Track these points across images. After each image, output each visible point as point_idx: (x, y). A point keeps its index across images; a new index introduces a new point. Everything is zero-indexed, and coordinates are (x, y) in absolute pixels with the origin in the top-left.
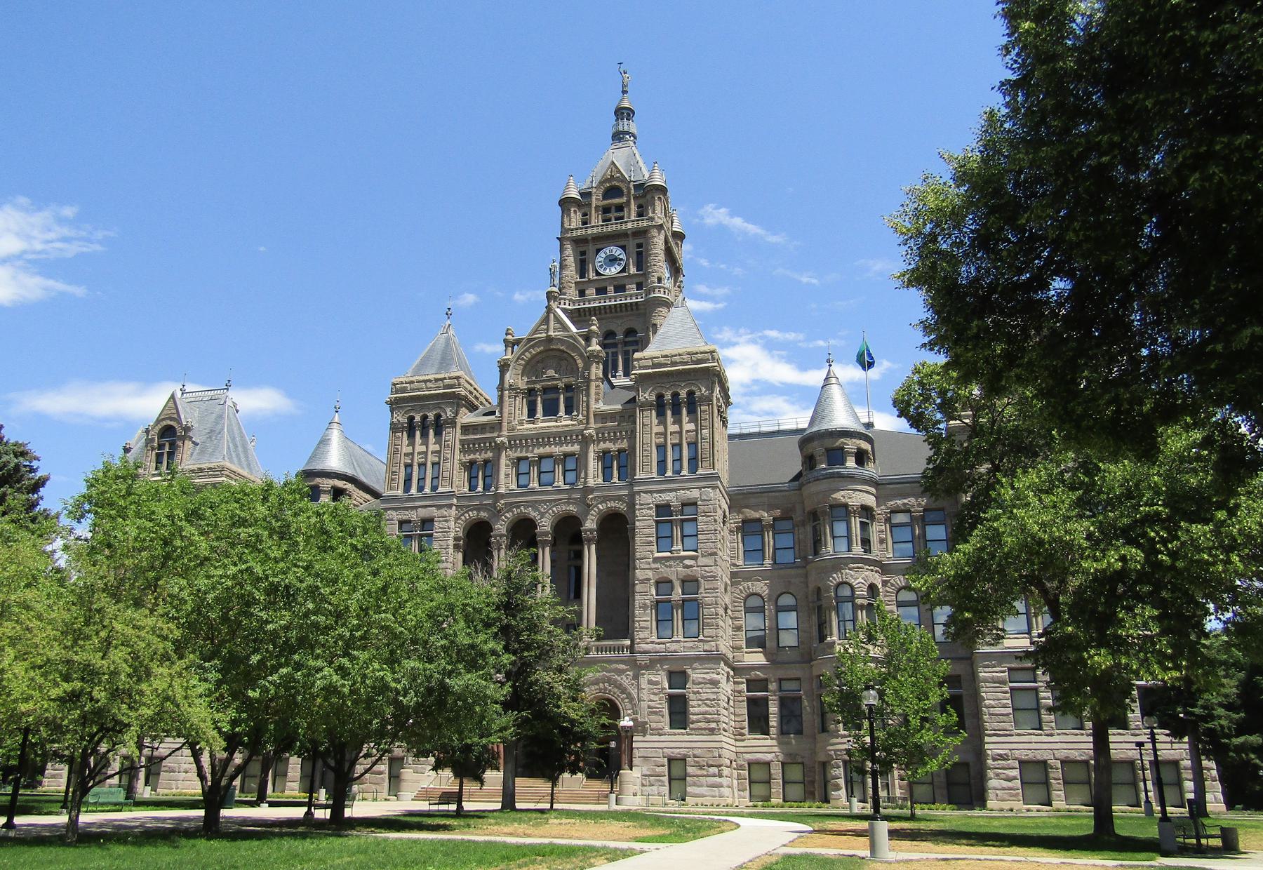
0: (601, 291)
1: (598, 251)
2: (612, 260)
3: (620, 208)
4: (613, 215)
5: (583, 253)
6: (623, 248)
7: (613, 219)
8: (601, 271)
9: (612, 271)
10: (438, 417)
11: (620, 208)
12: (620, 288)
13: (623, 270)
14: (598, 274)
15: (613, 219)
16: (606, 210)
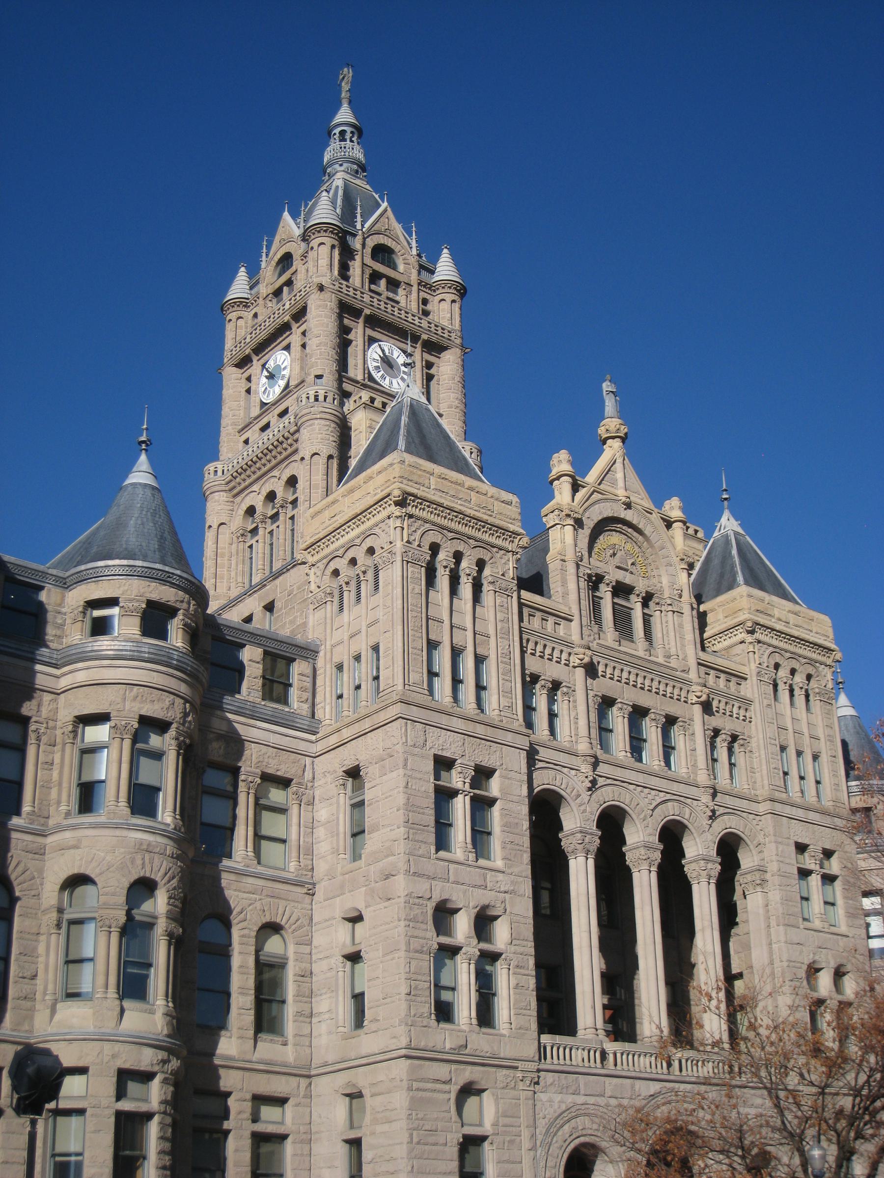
3: (393, 284)
8: (377, 376)
11: (393, 284)
14: (371, 378)
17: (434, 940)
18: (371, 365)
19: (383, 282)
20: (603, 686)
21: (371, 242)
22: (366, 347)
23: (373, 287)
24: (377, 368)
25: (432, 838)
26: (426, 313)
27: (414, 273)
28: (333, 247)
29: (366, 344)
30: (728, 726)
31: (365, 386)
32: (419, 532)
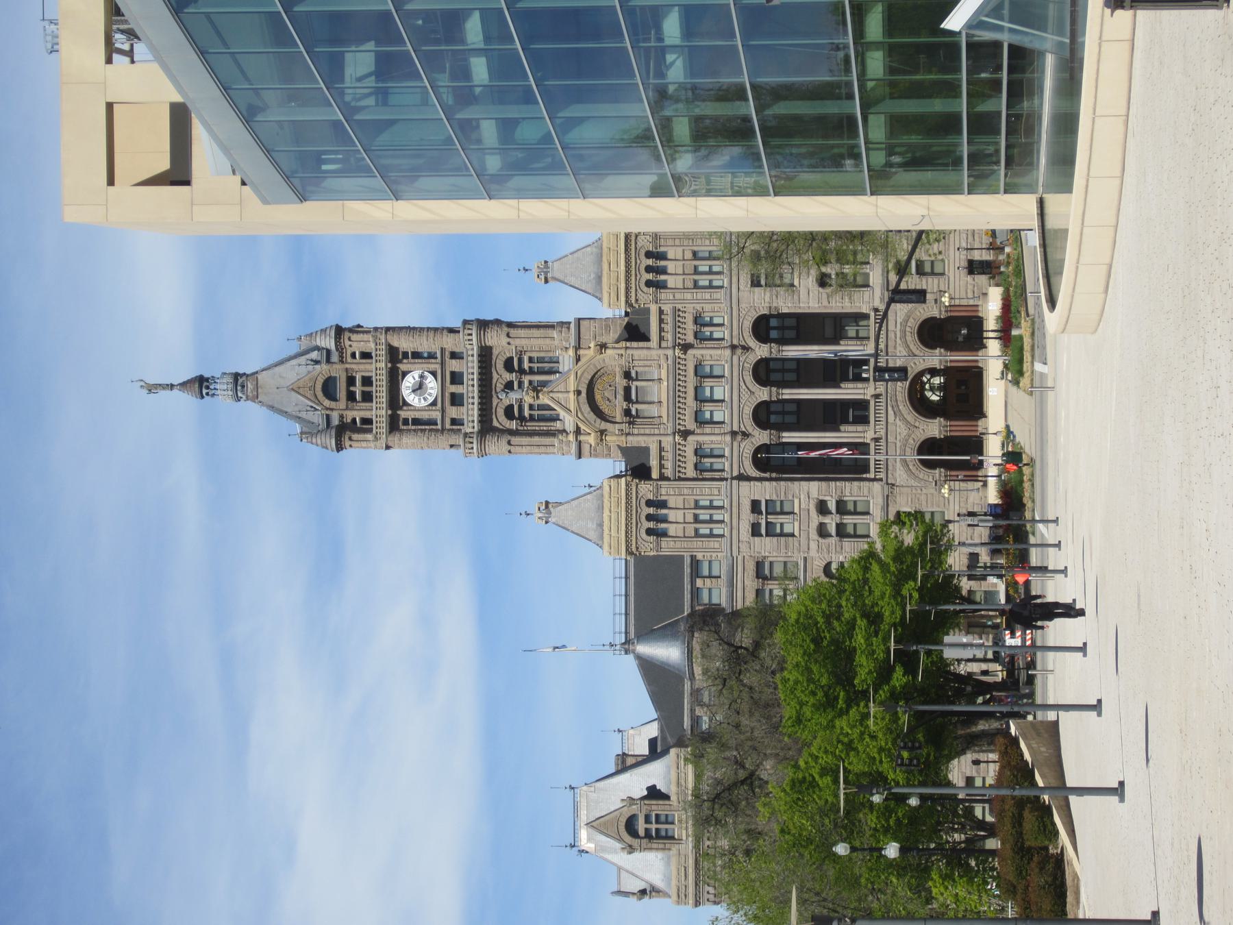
0: (456, 400)
1: (405, 403)
2: (419, 388)
3: (351, 381)
4: (358, 389)
5: (406, 422)
6: (405, 374)
7: (367, 389)
8: (431, 400)
9: (432, 385)
10: (649, 503)
11: (351, 381)
12: (456, 378)
13: (434, 374)
14: (434, 403)
15: (367, 389)
16: (351, 397)
17: (833, 540)
18: (424, 404)
19: (352, 389)
20: (690, 425)
21: (327, 403)
22: (412, 408)
23: (358, 397)
24: (425, 399)
25: (790, 539)
26: (366, 355)
27: (334, 366)
28: (350, 439)
29: (410, 408)
30: (690, 327)
31: (443, 411)
32: (644, 543)
